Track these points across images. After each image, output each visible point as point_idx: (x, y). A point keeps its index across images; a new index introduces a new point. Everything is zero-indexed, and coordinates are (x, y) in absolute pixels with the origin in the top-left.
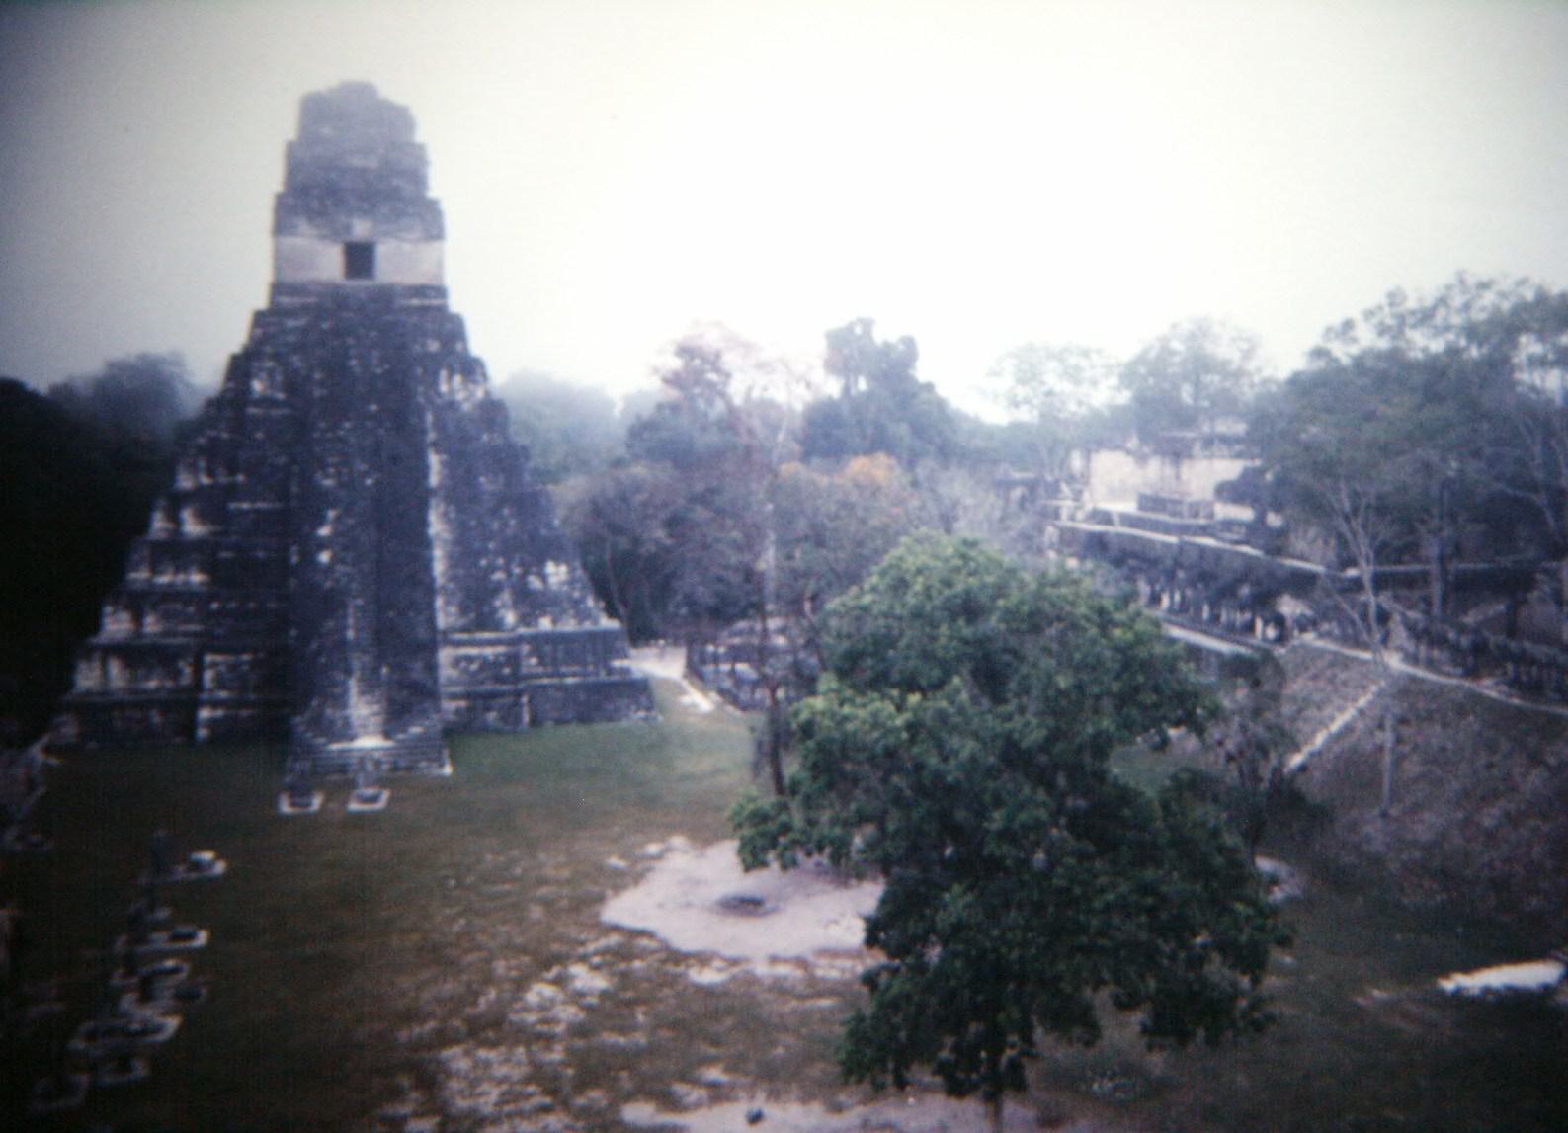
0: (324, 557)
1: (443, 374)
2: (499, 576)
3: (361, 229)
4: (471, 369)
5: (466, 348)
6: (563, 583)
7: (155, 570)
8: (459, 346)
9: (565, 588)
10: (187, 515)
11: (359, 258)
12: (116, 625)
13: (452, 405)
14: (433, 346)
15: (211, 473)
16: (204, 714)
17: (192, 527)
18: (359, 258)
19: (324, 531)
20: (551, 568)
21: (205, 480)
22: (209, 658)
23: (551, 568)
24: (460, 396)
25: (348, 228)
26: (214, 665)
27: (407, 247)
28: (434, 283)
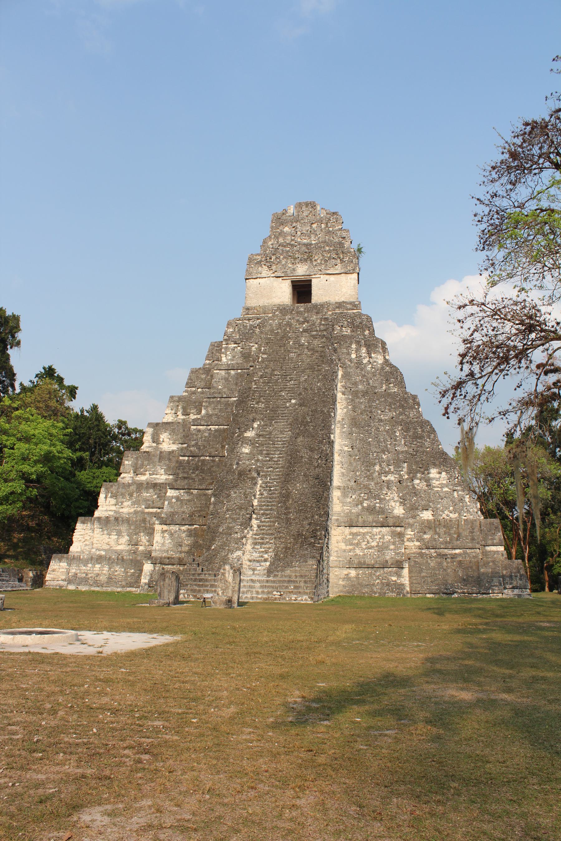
0: (246, 450)
1: (354, 346)
2: (391, 477)
3: (301, 271)
4: (374, 344)
5: (372, 332)
6: (442, 486)
7: (136, 473)
8: (367, 332)
9: (446, 489)
10: (164, 436)
11: (302, 290)
12: (106, 505)
13: (359, 364)
14: (347, 331)
15: (185, 413)
16: (148, 567)
17: (168, 444)
18: (302, 290)
19: (250, 434)
20: (433, 473)
21: (181, 417)
22: (158, 527)
23: (433, 473)
24: (365, 361)
25: (294, 270)
26: (163, 532)
27: (332, 278)
28: (352, 300)
